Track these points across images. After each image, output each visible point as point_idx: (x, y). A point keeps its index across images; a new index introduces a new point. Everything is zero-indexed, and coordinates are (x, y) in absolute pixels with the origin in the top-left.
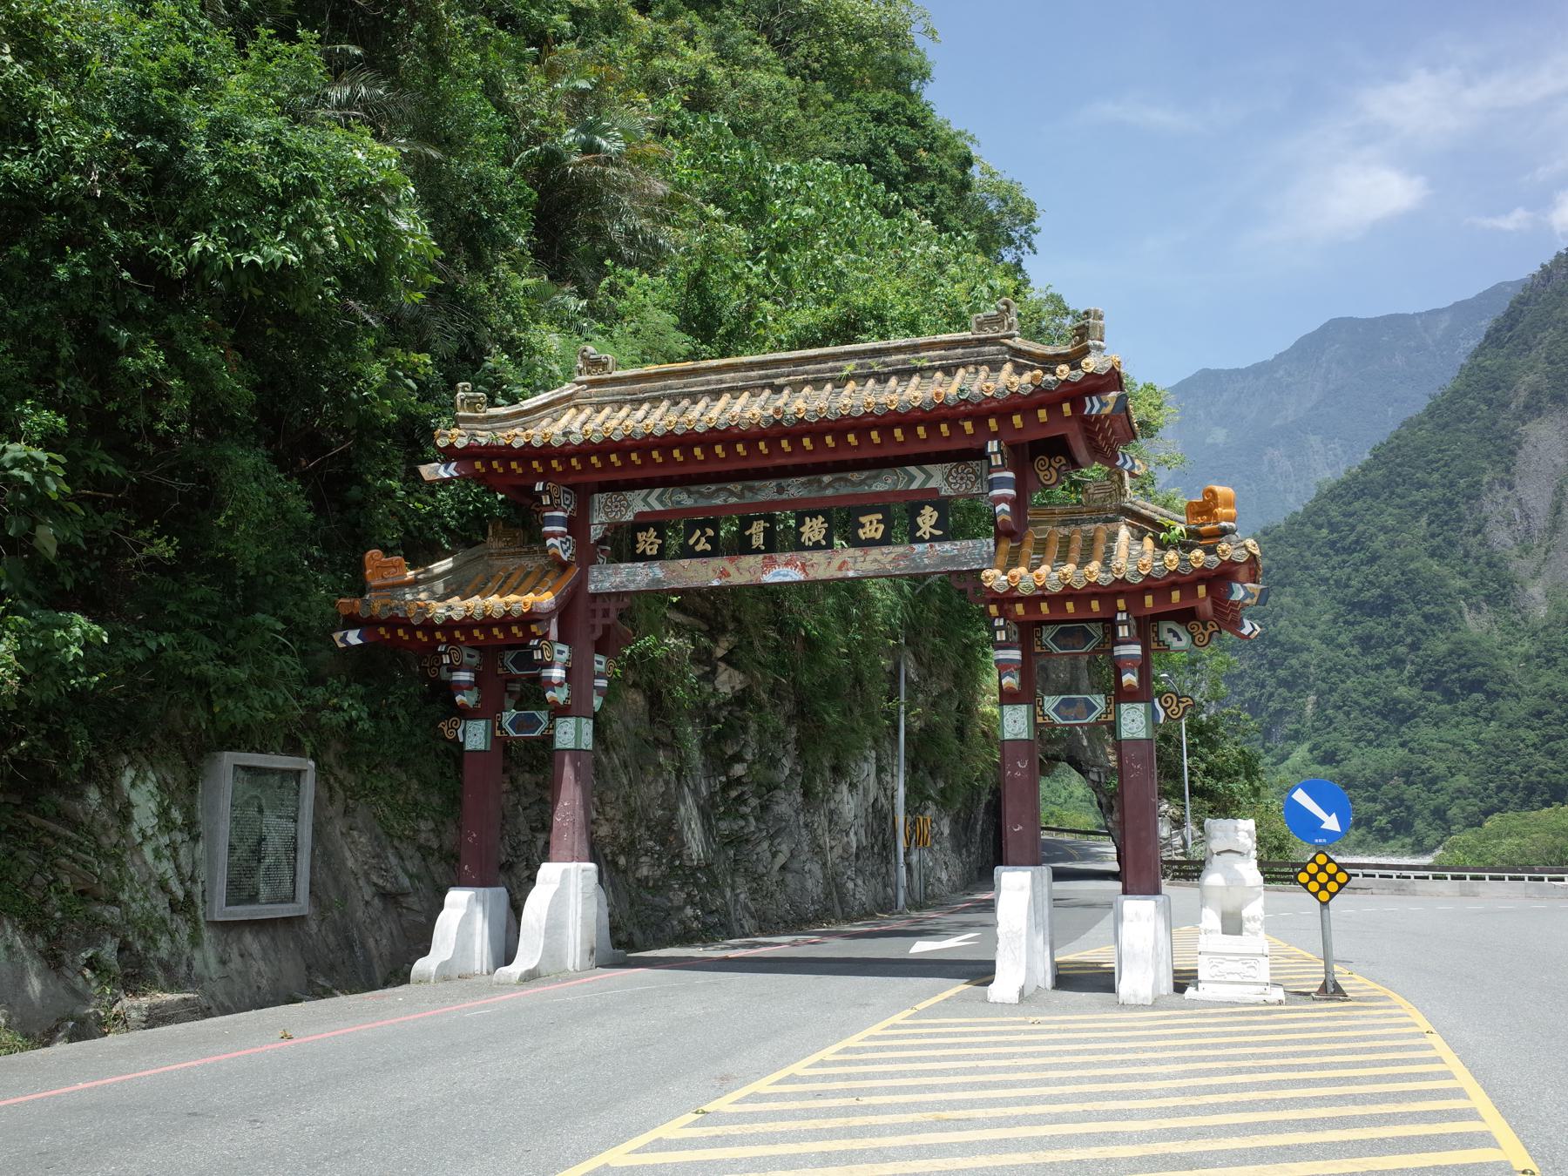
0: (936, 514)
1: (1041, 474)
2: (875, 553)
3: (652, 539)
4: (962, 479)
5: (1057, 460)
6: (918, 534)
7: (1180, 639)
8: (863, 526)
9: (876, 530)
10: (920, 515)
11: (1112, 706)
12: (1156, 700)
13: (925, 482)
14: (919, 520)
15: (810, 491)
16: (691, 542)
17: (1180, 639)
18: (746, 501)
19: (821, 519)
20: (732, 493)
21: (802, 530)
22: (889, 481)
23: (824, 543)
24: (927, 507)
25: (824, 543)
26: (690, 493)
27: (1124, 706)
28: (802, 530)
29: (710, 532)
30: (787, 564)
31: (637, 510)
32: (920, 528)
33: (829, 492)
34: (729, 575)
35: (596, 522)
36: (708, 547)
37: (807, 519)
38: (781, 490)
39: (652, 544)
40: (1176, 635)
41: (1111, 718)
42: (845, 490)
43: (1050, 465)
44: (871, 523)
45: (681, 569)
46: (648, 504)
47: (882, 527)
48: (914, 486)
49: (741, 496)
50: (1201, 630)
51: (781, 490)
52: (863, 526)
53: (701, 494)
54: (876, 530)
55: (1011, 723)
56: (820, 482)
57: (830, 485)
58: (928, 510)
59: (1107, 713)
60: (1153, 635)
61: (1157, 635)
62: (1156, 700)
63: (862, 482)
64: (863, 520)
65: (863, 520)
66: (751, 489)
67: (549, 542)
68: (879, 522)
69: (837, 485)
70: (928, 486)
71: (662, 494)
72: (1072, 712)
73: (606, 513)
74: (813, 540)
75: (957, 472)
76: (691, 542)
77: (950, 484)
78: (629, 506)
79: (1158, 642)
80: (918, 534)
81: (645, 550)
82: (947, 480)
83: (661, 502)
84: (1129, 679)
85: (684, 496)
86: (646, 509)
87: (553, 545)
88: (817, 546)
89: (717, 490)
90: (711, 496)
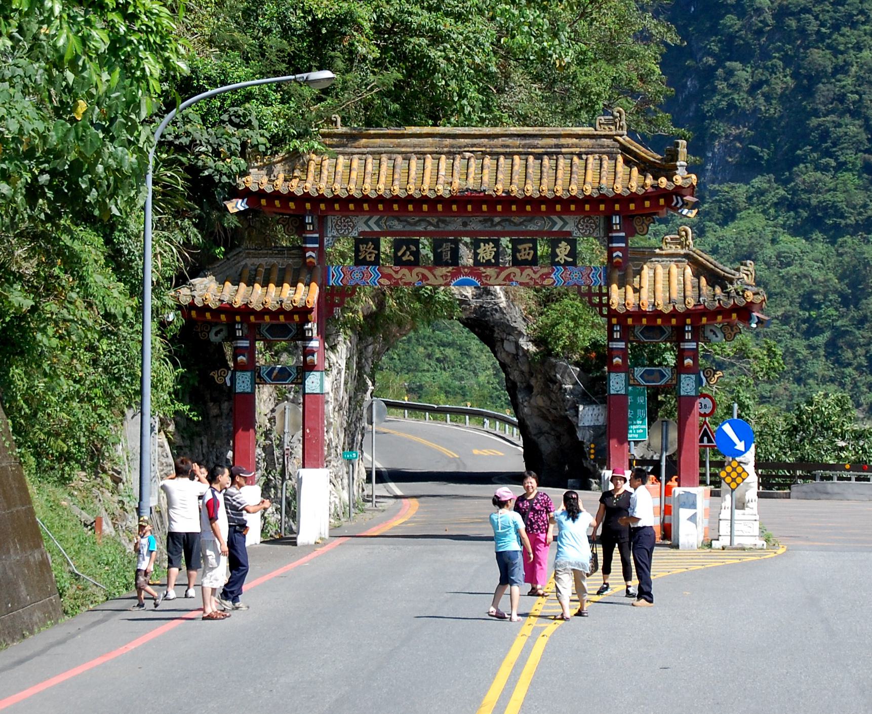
0: (569, 247)
1: (637, 228)
2: (528, 271)
3: (371, 250)
4: (587, 226)
5: (648, 219)
6: (557, 260)
7: (717, 336)
8: (519, 251)
9: (529, 254)
10: (558, 247)
11: (675, 375)
12: (702, 373)
13: (563, 226)
14: (558, 251)
15: (485, 227)
16: (400, 254)
17: (717, 336)
18: (440, 229)
19: (491, 245)
20: (430, 224)
21: (478, 251)
22: (539, 224)
23: (493, 261)
24: (563, 242)
25: (493, 261)
26: (399, 220)
27: (683, 376)
28: (478, 251)
29: (413, 248)
30: (467, 274)
31: (360, 229)
32: (558, 256)
33: (498, 228)
34: (427, 279)
35: (330, 235)
36: (412, 259)
37: (482, 244)
38: (465, 224)
39: (370, 253)
40: (715, 333)
41: (674, 382)
42: (509, 228)
43: (643, 223)
44: (525, 249)
45: (393, 274)
46: (369, 227)
47: (532, 252)
48: (556, 229)
49: (437, 226)
50: (730, 331)
51: (465, 224)
52: (519, 251)
53: (409, 223)
54: (529, 254)
55: (615, 384)
56: (492, 221)
57: (499, 223)
58: (563, 244)
59: (671, 379)
60: (701, 333)
61: (704, 333)
62: (702, 373)
63: (521, 224)
64: (520, 247)
65: (520, 247)
66: (444, 222)
67: (308, 254)
68: (530, 249)
69: (503, 224)
70: (564, 230)
71: (379, 220)
72: (650, 378)
73: (337, 230)
74: (486, 259)
75: (584, 222)
76: (400, 254)
77: (579, 229)
78: (354, 226)
79: (704, 337)
80: (557, 260)
81: (365, 257)
82: (577, 226)
83: (379, 226)
84: (688, 362)
85: (396, 223)
86: (368, 230)
87: (311, 256)
88: (488, 264)
89: (419, 221)
90: (415, 224)
